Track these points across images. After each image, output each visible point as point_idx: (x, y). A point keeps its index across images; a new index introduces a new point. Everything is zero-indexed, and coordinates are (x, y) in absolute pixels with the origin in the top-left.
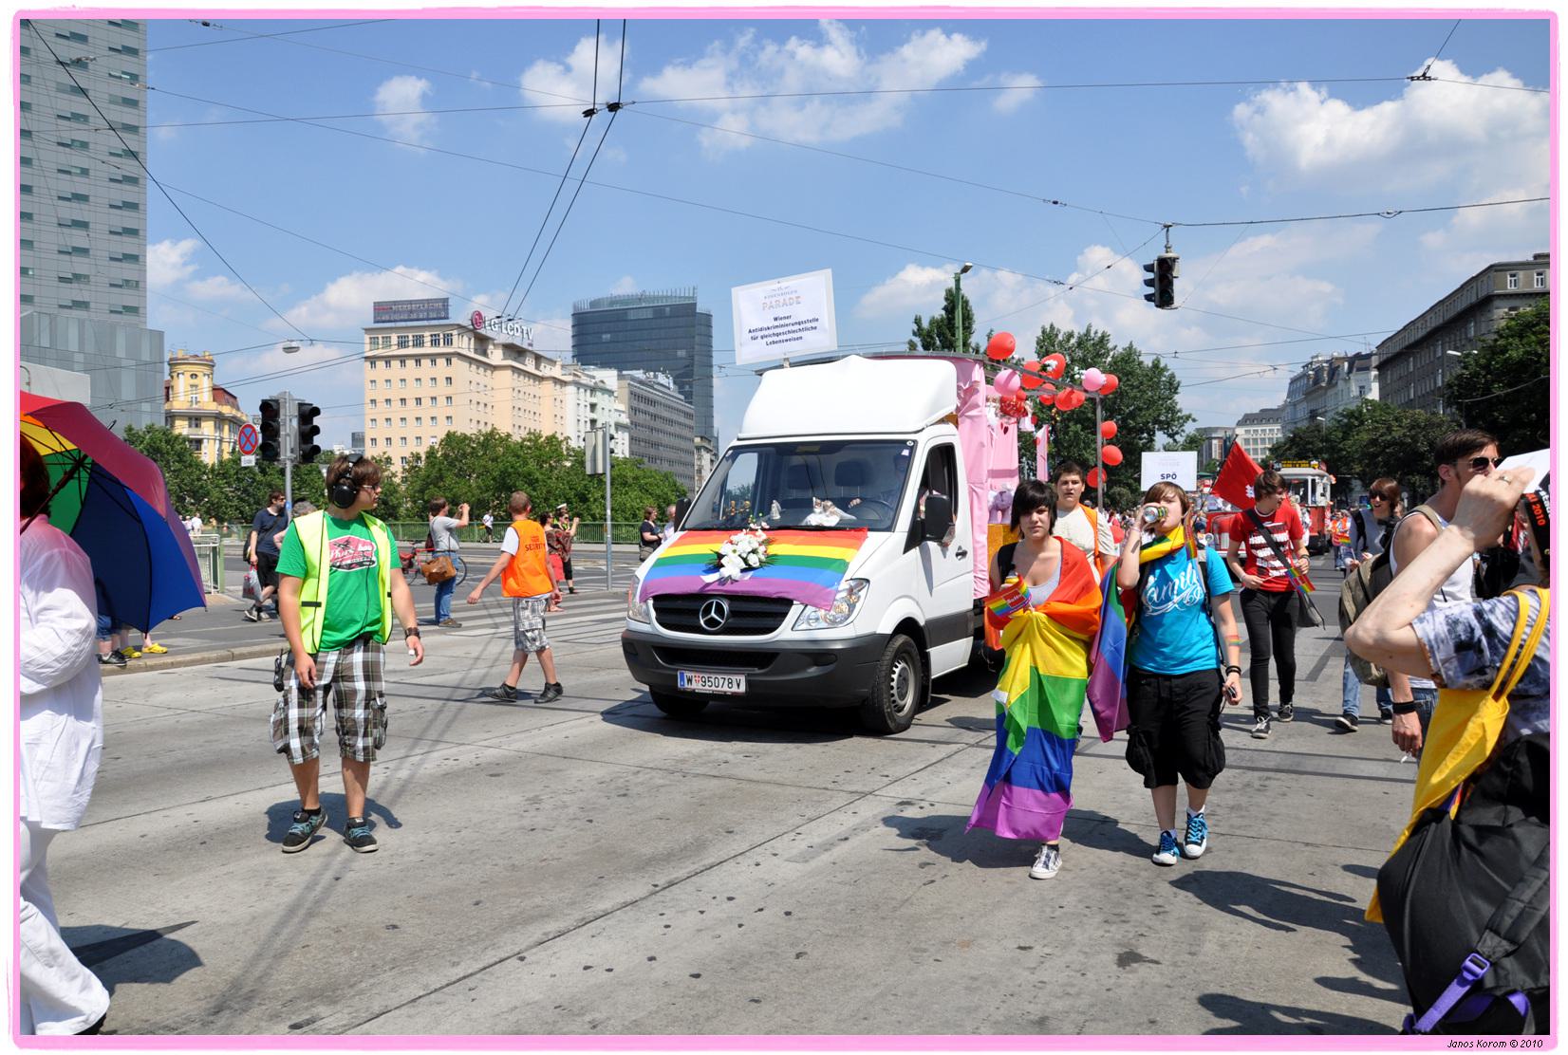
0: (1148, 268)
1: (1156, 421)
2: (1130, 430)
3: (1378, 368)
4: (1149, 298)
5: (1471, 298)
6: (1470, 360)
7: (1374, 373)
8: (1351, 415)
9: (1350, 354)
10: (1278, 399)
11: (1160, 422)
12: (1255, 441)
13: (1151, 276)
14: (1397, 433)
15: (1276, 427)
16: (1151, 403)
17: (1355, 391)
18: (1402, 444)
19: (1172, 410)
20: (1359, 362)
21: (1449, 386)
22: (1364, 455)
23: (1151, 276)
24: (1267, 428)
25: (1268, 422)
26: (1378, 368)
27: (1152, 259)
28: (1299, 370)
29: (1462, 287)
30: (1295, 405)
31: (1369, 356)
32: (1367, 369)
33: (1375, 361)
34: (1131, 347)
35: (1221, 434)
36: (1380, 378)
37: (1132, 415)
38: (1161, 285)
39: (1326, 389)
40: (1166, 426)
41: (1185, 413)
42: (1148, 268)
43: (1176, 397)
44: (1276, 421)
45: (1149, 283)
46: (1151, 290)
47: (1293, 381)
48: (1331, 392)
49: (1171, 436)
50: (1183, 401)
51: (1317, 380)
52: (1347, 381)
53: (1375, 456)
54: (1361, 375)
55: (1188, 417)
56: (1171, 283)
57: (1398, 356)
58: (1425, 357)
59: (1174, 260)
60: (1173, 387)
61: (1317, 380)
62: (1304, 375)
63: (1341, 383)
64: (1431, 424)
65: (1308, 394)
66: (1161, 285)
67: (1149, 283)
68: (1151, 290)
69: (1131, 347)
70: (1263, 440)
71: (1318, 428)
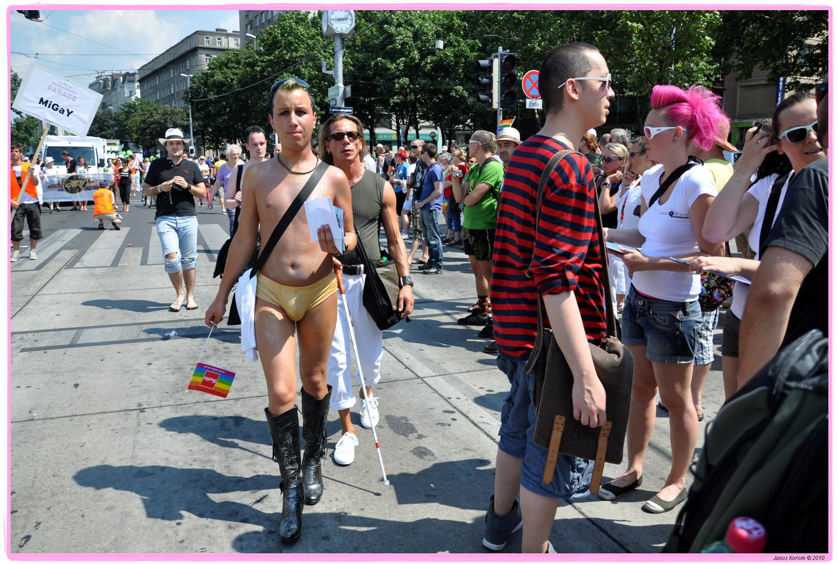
3: (140, 81)
7: (137, 84)
9: (123, 72)
14: (157, 117)
17: (127, 94)
18: (159, 123)
20: (128, 77)
21: (186, 92)
22: (139, 129)
26: (140, 81)
31: (134, 74)
32: (133, 81)
33: (137, 77)
36: (141, 87)
39: (110, 91)
48: (113, 93)
51: (105, 86)
52: (123, 87)
53: (144, 130)
54: (130, 85)
57: (152, 75)
58: (164, 78)
64: (173, 113)
71: (110, 113)
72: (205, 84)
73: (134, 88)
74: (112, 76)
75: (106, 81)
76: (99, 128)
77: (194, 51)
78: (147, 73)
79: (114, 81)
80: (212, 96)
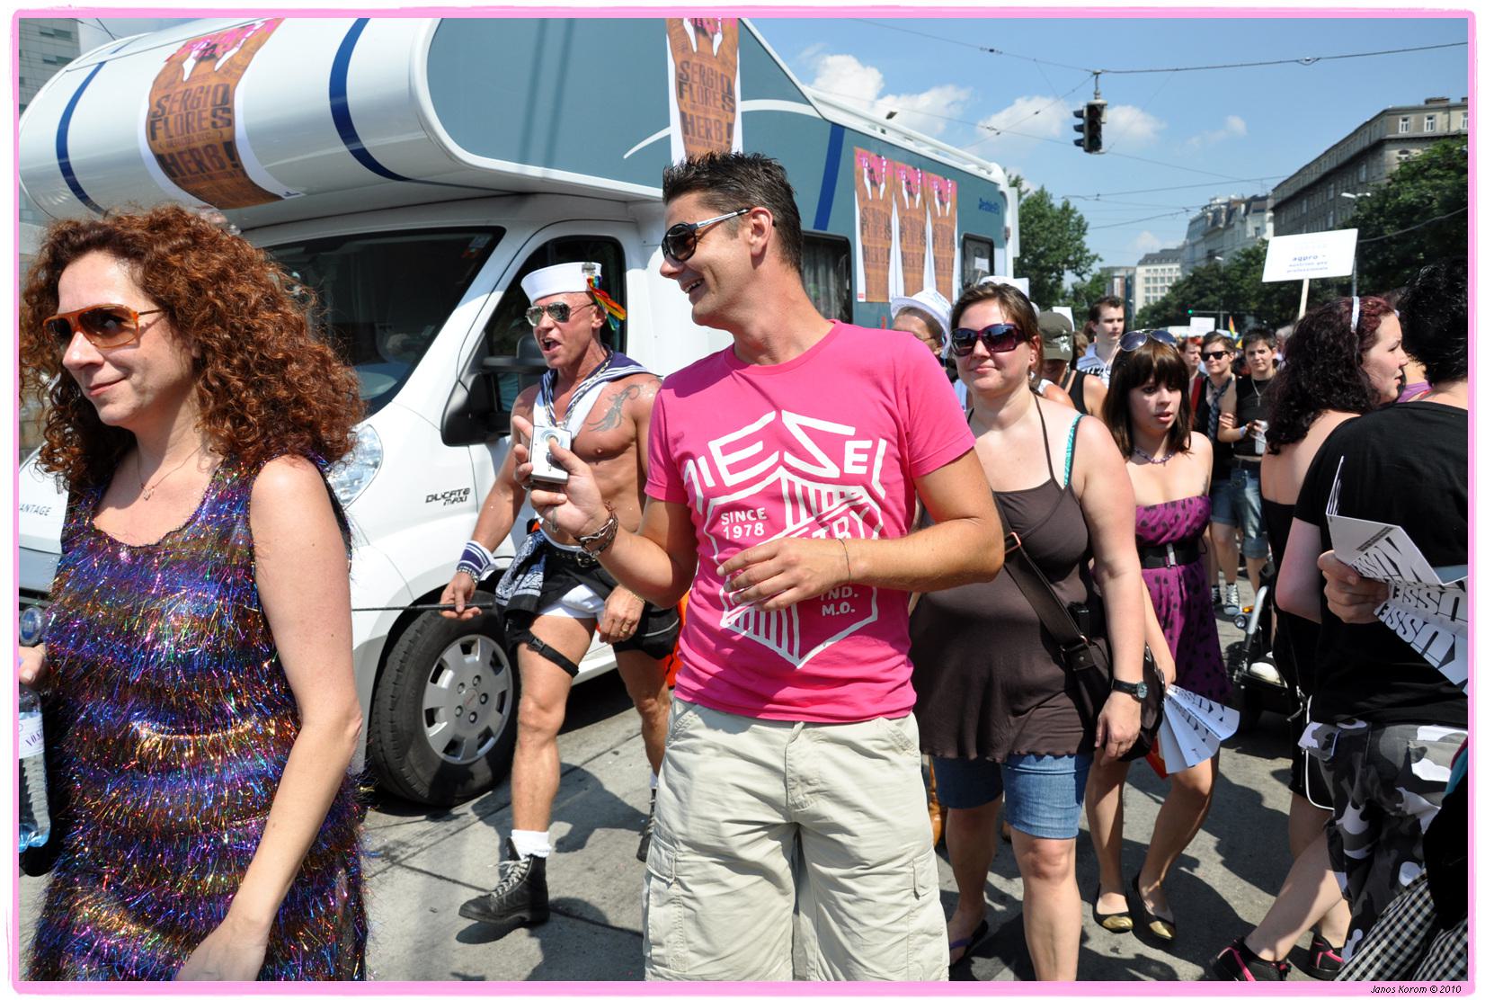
0: (1078, 114)
1: (1066, 261)
2: (1042, 269)
4: (1078, 143)
5: (1364, 142)
6: (1365, 203)
7: (1270, 214)
8: (1248, 255)
9: (1248, 196)
10: (1176, 237)
11: (1066, 261)
12: (1155, 279)
13: (1080, 121)
15: (1177, 266)
16: (1060, 245)
17: (1251, 232)
19: (1080, 250)
20: (1254, 205)
23: (1080, 121)
24: (1167, 267)
25: (1167, 261)
26: (1274, 209)
27: (1081, 106)
28: (1197, 213)
29: (1356, 132)
30: (1193, 245)
31: (1265, 198)
32: (1263, 211)
33: (1270, 203)
34: (1042, 189)
35: (1122, 273)
36: (1275, 219)
37: (1042, 255)
38: (1090, 129)
40: (1074, 266)
41: (1093, 252)
42: (1078, 114)
43: (1085, 238)
44: (1175, 261)
45: (1079, 129)
46: (1080, 136)
47: (1193, 223)
48: (1228, 233)
49: (1079, 275)
50: (1091, 242)
51: (1215, 221)
52: (1243, 222)
55: (1095, 257)
56: (1099, 129)
59: (1102, 106)
60: (1081, 228)
61: (1215, 223)
62: (1203, 217)
63: (1238, 226)
65: (1205, 235)
66: (1090, 129)
67: (1079, 129)
68: (1080, 136)
69: (1042, 189)
70: (1163, 279)
71: (1217, 263)
72: (1381, 210)
73: (1263, 222)
74: (1228, 204)
75: (1217, 213)
76: (1197, 293)
77: (1378, 146)
78: (1288, 193)
79: (1231, 212)
80: (1390, 232)
